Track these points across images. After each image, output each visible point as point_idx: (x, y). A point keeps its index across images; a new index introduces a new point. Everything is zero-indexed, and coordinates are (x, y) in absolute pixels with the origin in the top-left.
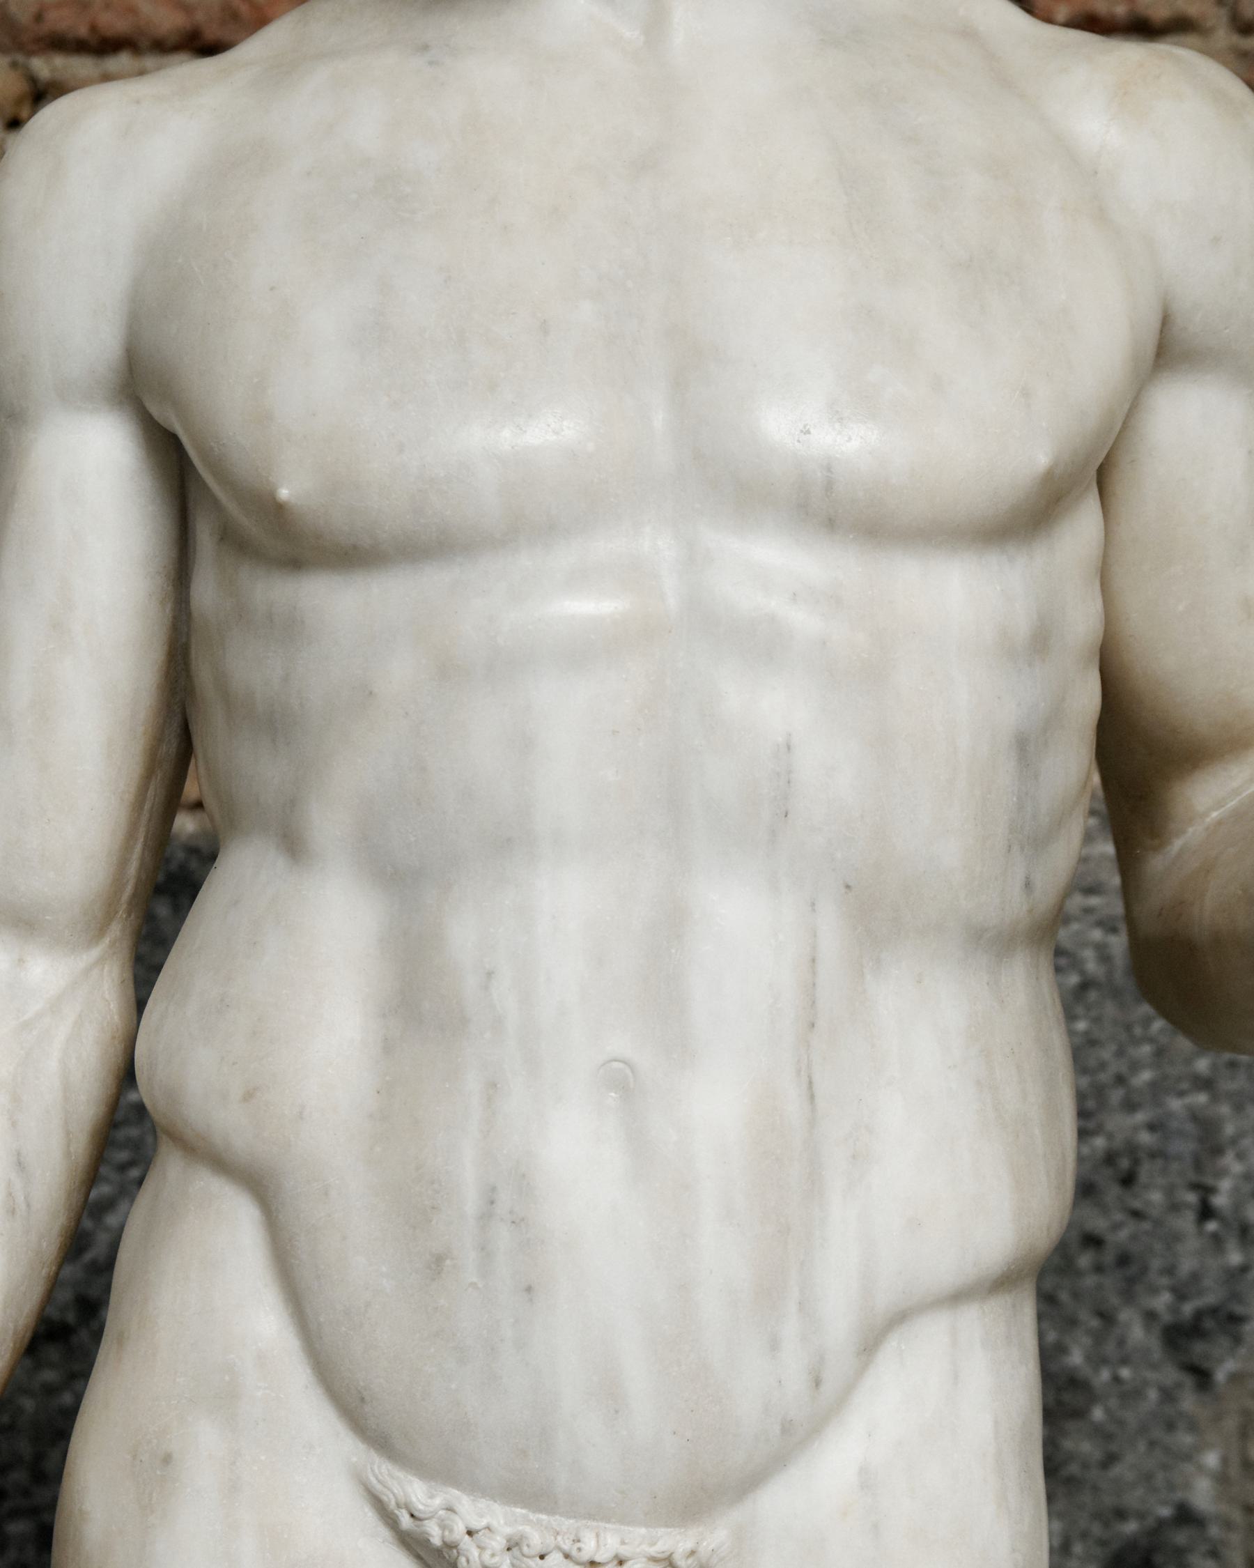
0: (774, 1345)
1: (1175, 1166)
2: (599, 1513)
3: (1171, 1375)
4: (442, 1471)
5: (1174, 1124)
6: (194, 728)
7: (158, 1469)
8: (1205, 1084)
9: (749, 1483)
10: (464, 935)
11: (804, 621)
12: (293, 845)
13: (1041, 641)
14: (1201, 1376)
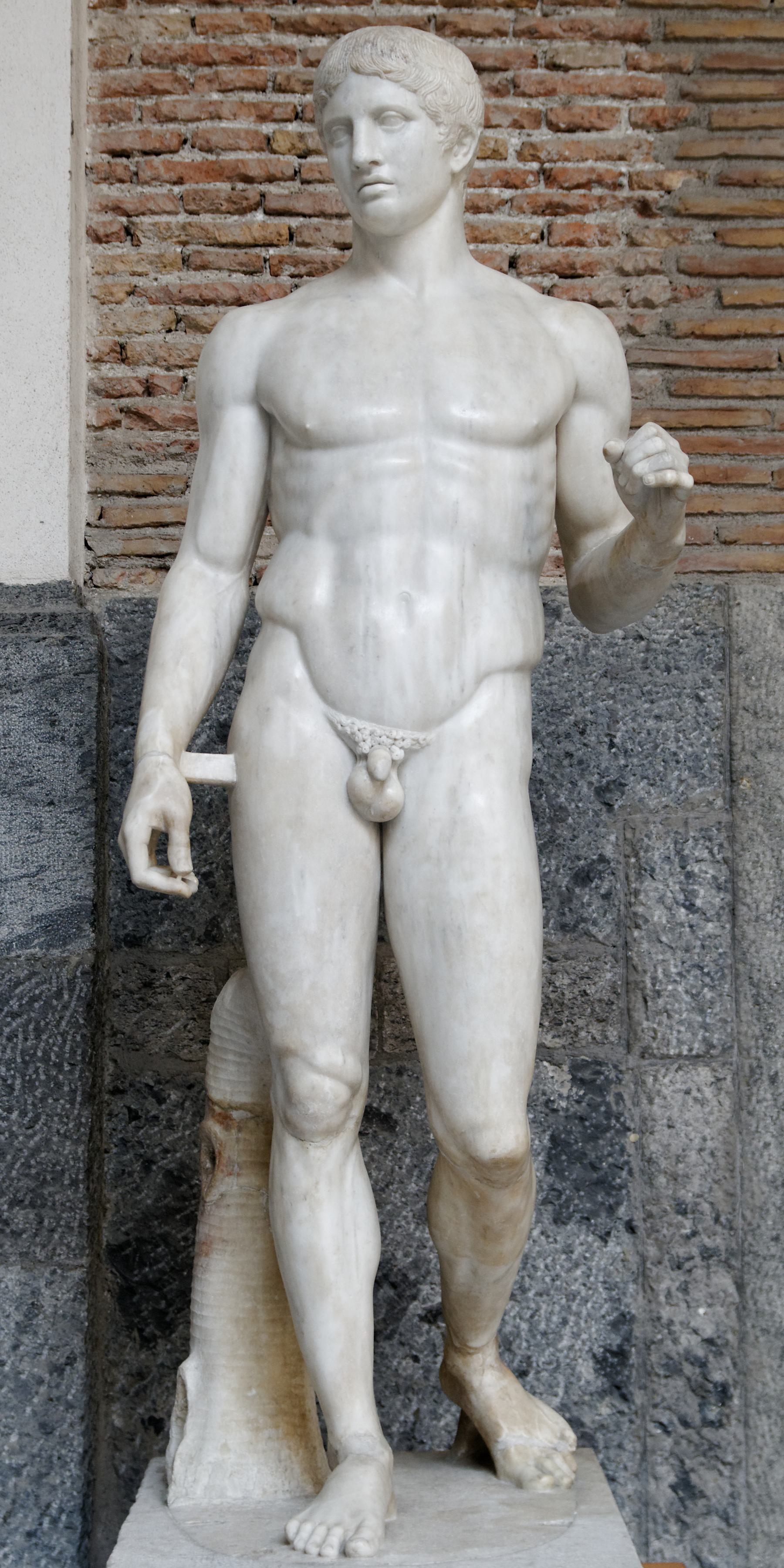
0: (450, 678)
1: (601, 727)
2: (397, 726)
3: (598, 806)
4: (351, 712)
5: (600, 711)
6: (272, 508)
7: (265, 714)
8: (613, 697)
9: (442, 720)
10: (360, 556)
11: (463, 467)
12: (308, 531)
13: (534, 478)
14: (609, 806)
